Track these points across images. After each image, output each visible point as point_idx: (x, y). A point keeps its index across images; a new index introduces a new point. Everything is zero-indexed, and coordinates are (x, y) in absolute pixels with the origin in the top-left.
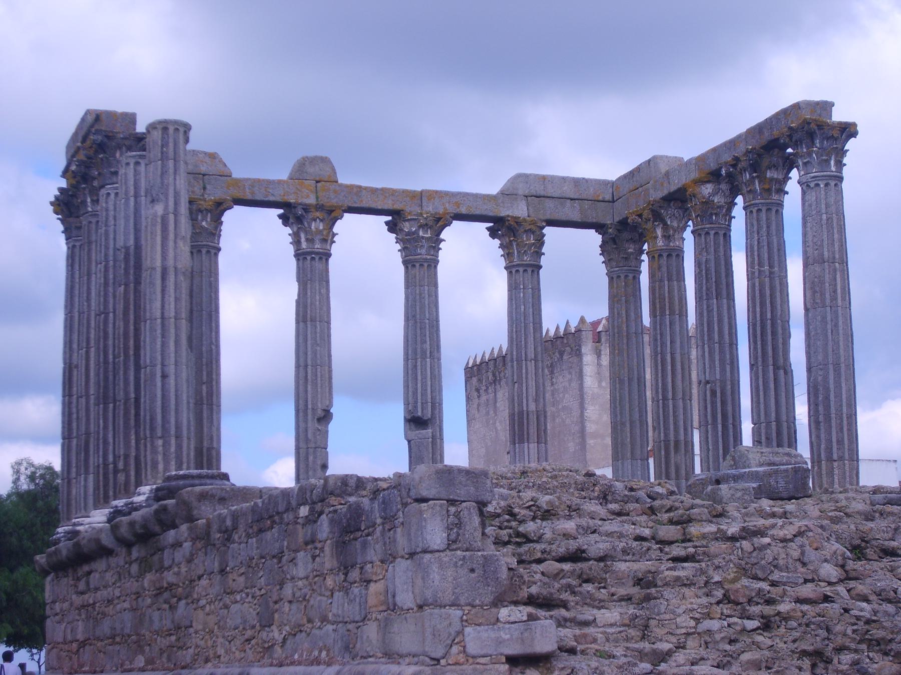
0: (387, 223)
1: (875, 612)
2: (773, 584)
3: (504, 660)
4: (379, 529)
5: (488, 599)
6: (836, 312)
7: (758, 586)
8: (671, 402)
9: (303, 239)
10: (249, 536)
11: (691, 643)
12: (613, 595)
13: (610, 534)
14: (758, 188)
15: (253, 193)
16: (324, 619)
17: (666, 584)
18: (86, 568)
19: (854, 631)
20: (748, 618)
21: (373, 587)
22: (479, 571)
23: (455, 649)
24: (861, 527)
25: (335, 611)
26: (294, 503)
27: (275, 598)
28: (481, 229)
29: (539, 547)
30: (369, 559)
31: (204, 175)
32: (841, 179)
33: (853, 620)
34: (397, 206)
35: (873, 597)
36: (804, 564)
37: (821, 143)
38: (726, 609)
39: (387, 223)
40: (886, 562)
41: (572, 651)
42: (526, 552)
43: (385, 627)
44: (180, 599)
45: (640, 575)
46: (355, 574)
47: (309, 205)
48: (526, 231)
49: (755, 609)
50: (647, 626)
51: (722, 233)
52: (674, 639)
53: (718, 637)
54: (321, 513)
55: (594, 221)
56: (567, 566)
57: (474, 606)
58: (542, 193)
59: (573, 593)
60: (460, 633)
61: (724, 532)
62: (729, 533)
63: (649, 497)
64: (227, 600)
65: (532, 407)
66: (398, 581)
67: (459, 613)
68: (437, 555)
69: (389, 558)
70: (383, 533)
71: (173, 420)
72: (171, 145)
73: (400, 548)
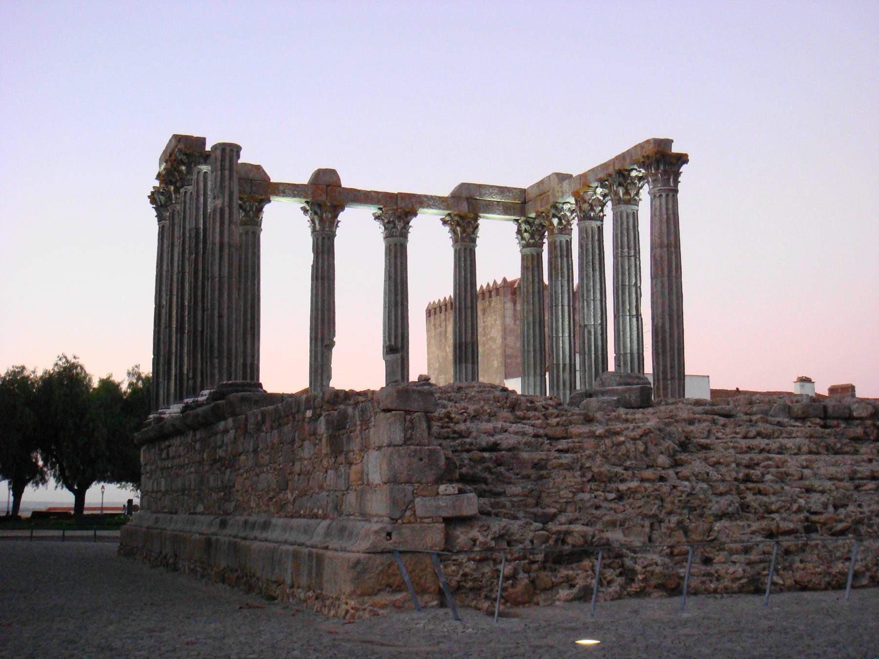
1: (693, 488)
2: (626, 469)
3: (441, 520)
4: (359, 428)
5: (431, 478)
7: (615, 470)
10: (272, 428)
12: (517, 474)
13: (517, 433)
16: (321, 488)
17: (554, 468)
18: (167, 443)
19: (680, 501)
20: (609, 492)
21: (353, 467)
22: (426, 460)
23: (408, 513)
24: (686, 429)
25: (328, 482)
26: (303, 408)
27: (288, 471)
29: (468, 440)
32: (677, 191)
33: (679, 494)
36: (647, 455)
37: (664, 167)
38: (593, 485)
40: (701, 454)
41: (488, 514)
42: (459, 445)
43: (361, 497)
44: (226, 468)
45: (536, 461)
46: (341, 458)
49: (613, 486)
50: (539, 497)
52: (558, 506)
53: (588, 504)
54: (320, 415)
56: (486, 455)
57: (422, 484)
59: (491, 473)
60: (412, 501)
61: (594, 433)
62: (597, 433)
63: (543, 407)
64: (257, 470)
67: (411, 488)
68: (397, 448)
69: (365, 448)
70: (361, 430)
71: (225, 346)
73: (372, 441)
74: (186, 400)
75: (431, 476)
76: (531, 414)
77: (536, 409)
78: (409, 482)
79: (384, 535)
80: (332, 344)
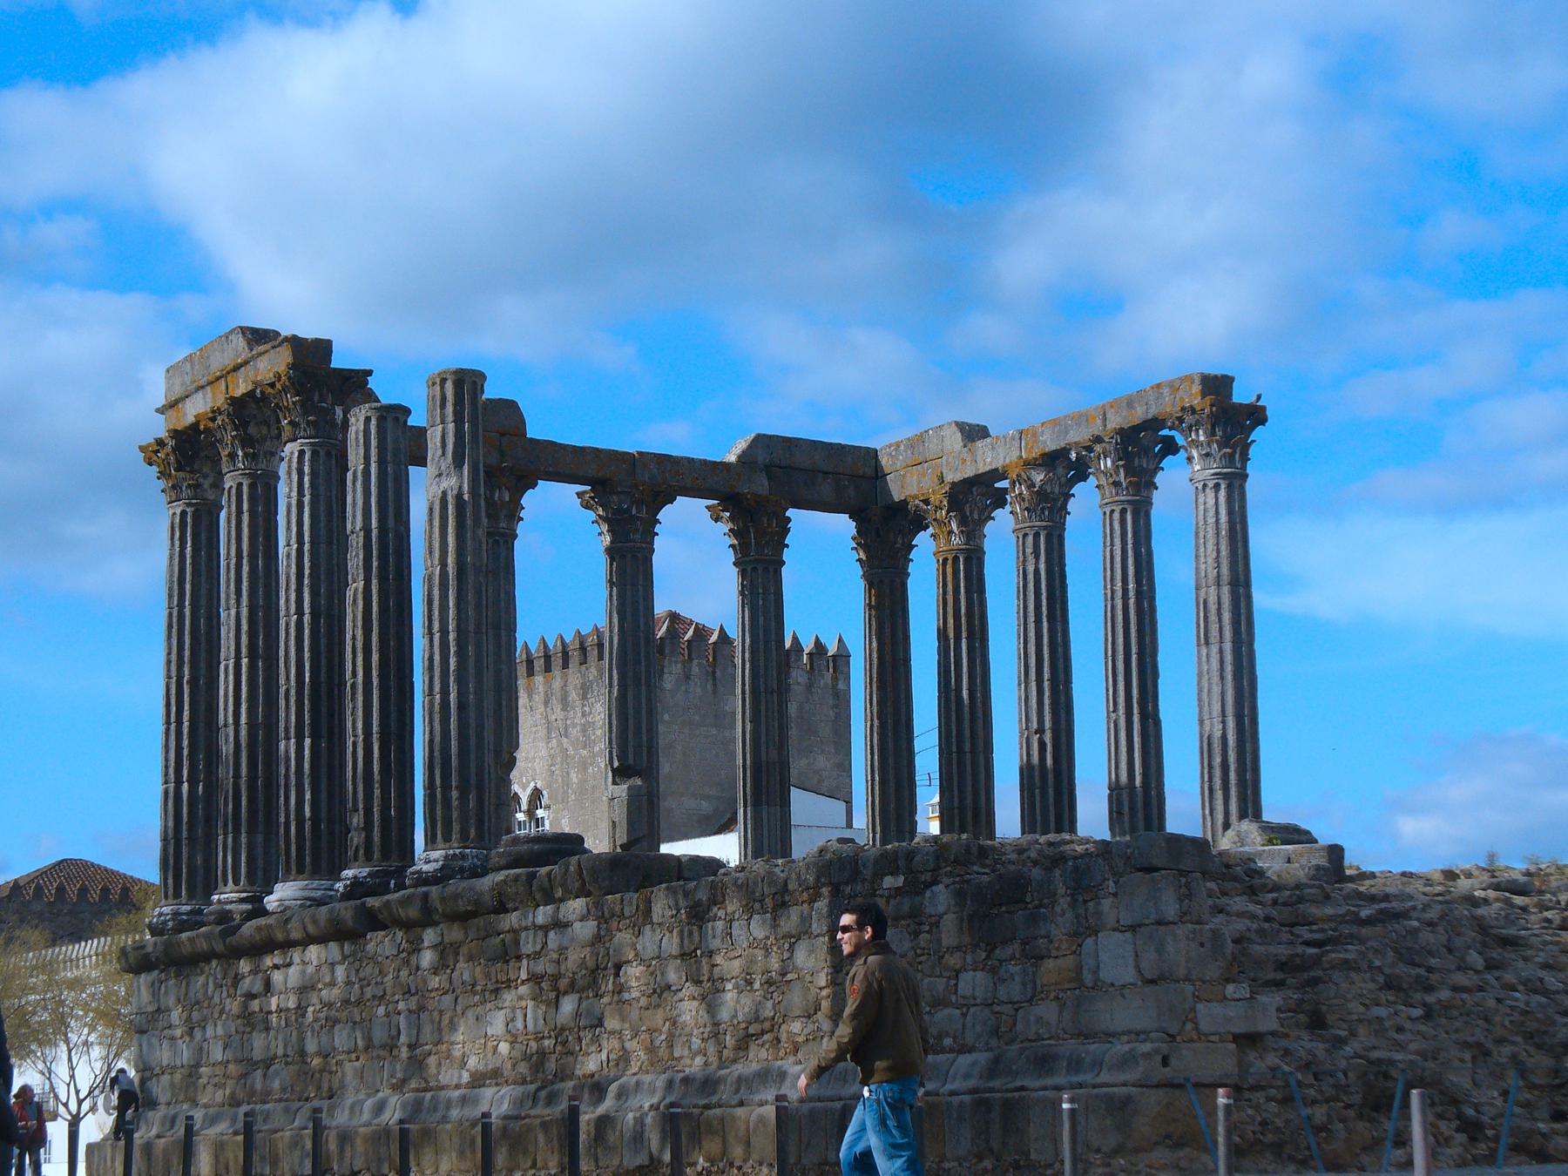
0: (579, 495)
1: (1527, 1004)
2: (1430, 970)
4: (1063, 903)
8: (968, 756)
11: (1362, 1031)
17: (1333, 967)
23: (1189, 1026)
30: (1043, 932)
35: (1521, 988)
39: (579, 495)
45: (1284, 959)
54: (935, 882)
60: (1193, 1009)
61: (1356, 914)
65: (774, 755)
66: (1103, 956)
69: (1087, 929)
74: (349, 873)
75: (1213, 971)
76: (1228, 885)
77: (1235, 878)
78: (1187, 979)
79: (1159, 1058)
80: (512, 762)
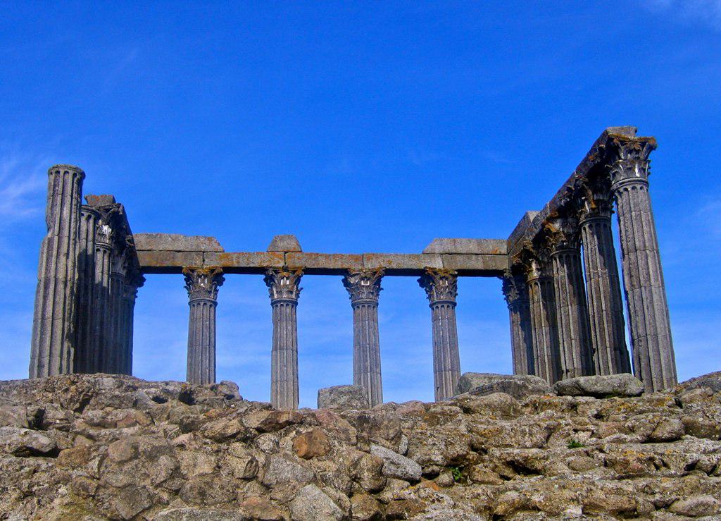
6: (651, 291)
9: (275, 292)
14: (588, 209)
15: (238, 262)
28: (414, 280)
31: (204, 252)
34: (345, 266)
37: (626, 155)
47: (278, 268)
48: (441, 278)
51: (572, 255)
55: (494, 268)
58: (454, 251)
72: (61, 184)
76: (120, 414)
